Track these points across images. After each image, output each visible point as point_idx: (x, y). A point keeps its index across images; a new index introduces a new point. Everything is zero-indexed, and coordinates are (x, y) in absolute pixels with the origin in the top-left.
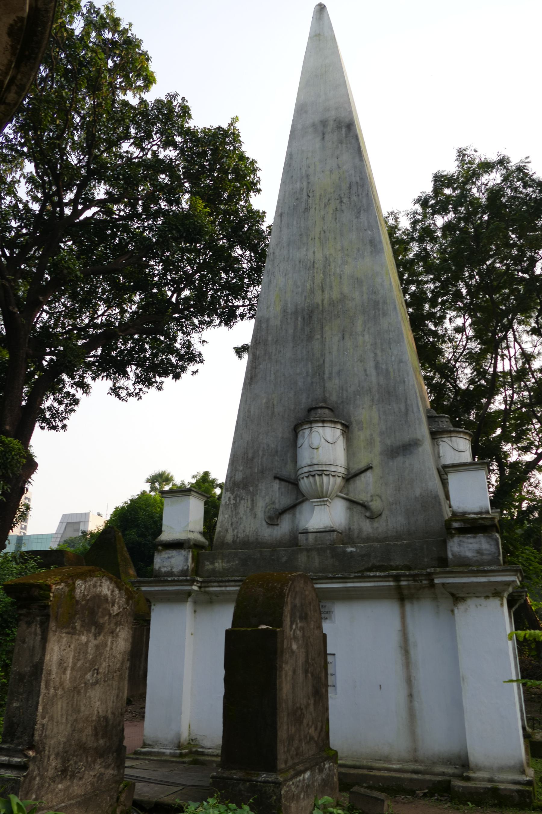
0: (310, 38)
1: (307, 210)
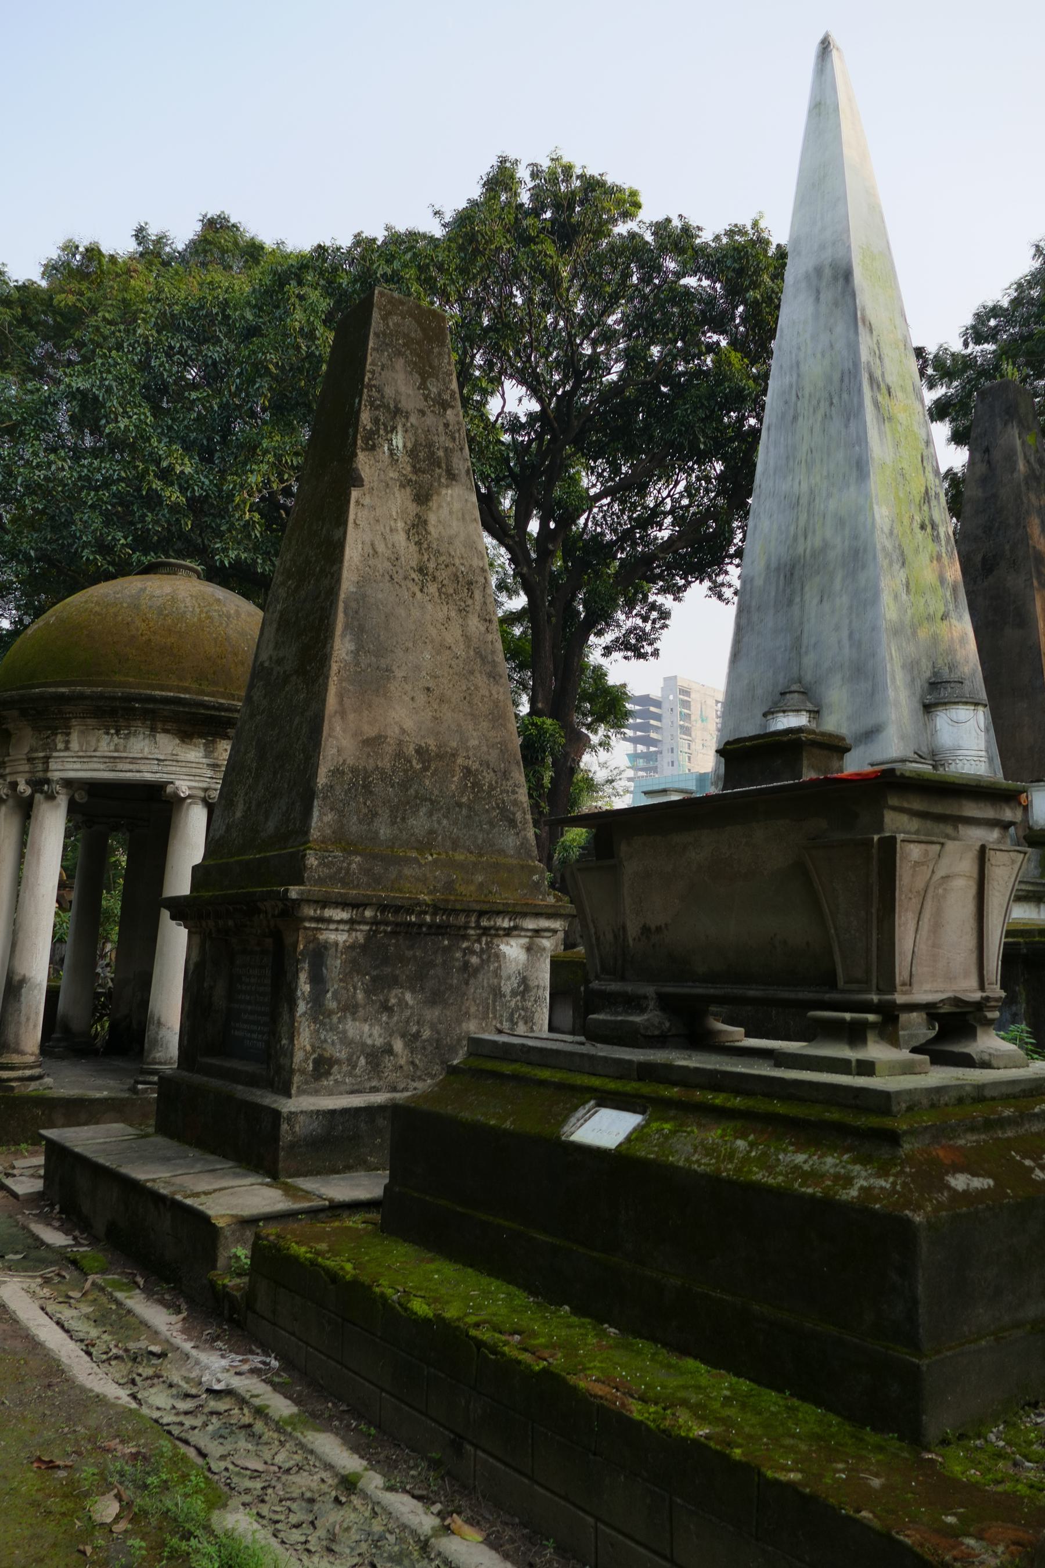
0: (810, 111)
1: (795, 418)
